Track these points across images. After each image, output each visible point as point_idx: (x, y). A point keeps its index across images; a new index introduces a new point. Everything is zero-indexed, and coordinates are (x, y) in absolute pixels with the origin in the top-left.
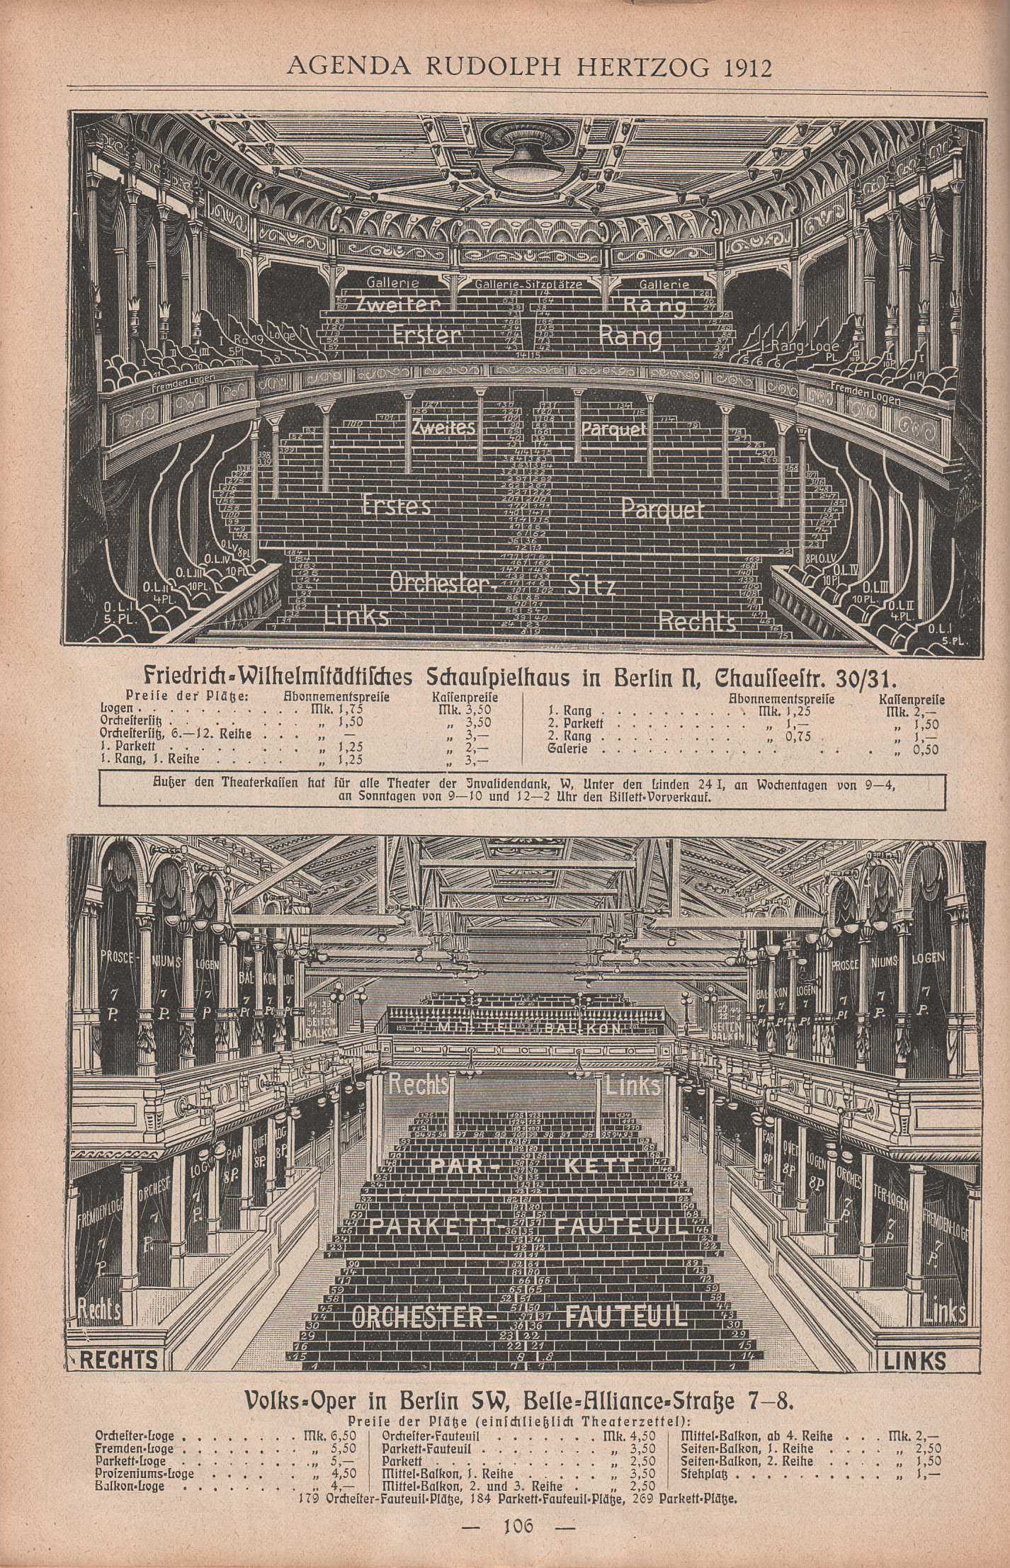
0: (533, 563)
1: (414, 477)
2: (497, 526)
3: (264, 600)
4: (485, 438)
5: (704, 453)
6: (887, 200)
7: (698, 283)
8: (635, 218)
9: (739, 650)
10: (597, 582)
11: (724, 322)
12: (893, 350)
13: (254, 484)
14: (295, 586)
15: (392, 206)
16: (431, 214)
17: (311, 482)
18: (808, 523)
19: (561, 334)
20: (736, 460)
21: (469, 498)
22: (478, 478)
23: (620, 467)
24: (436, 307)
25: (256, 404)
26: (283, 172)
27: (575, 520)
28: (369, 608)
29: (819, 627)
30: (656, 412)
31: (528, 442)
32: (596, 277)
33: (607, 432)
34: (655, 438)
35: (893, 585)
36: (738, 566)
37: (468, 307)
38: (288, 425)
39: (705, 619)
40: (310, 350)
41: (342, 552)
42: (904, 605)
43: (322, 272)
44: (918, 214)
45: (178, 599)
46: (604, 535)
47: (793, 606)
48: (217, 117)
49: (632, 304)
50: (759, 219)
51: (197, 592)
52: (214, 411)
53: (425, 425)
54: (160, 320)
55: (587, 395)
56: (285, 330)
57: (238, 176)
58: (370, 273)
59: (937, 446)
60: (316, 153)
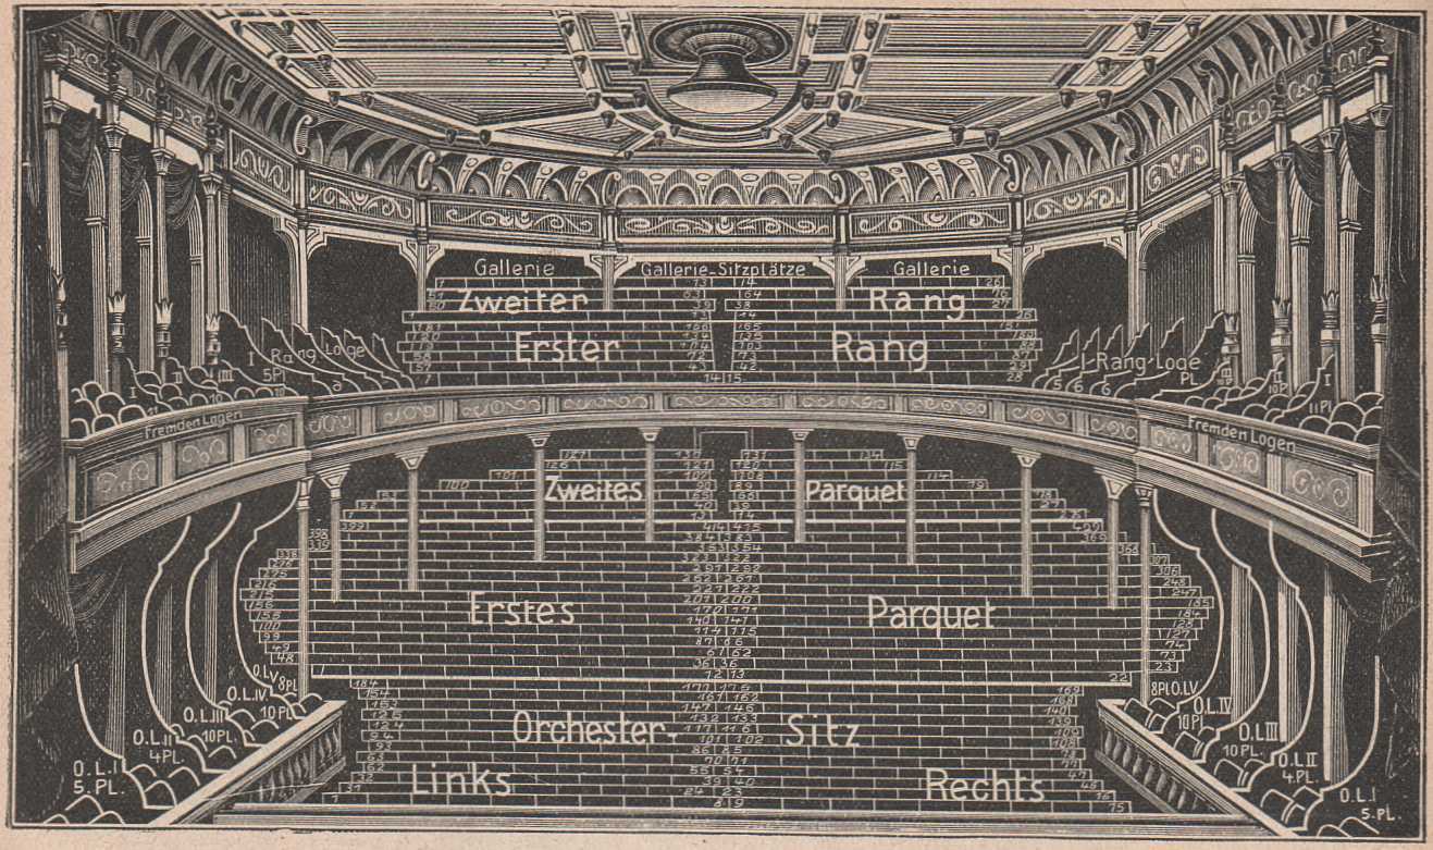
0: (731, 697)
1: (547, 567)
2: (677, 641)
3: (318, 757)
4: (657, 506)
5: (994, 527)
6: (1272, 138)
7: (983, 265)
8: (886, 167)
9: (1050, 830)
10: (830, 726)
11: (1024, 325)
12: (1283, 367)
13: (303, 579)
14: (367, 736)
15: (512, 150)
16: (573, 162)
17: (390, 575)
18: (1154, 634)
19: (774, 346)
20: (1042, 538)
21: (632, 599)
22: (647, 567)
23: (867, 553)
24: (581, 305)
25: (305, 455)
26: (345, 99)
27: (796, 631)
28: (481, 769)
29: (1172, 794)
30: (921, 463)
31: (723, 512)
32: (827, 257)
33: (844, 495)
34: (918, 505)
35: (1284, 728)
36: (1047, 700)
37: (630, 305)
38: (354, 487)
39: (996, 782)
40: (387, 372)
41: (438, 683)
42: (1303, 760)
43: (406, 252)
44: (1320, 158)
45: (186, 756)
46: (842, 654)
47: (1132, 762)
48: (242, 14)
49: (882, 299)
50: (1076, 167)
51: (215, 745)
52: (241, 466)
53: (564, 486)
54: (158, 328)
55: (814, 439)
56: (350, 342)
57: (276, 106)
58: (479, 254)
59: (1351, 514)
60: (396, 69)
